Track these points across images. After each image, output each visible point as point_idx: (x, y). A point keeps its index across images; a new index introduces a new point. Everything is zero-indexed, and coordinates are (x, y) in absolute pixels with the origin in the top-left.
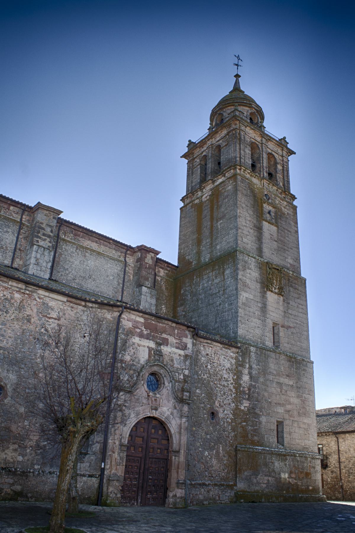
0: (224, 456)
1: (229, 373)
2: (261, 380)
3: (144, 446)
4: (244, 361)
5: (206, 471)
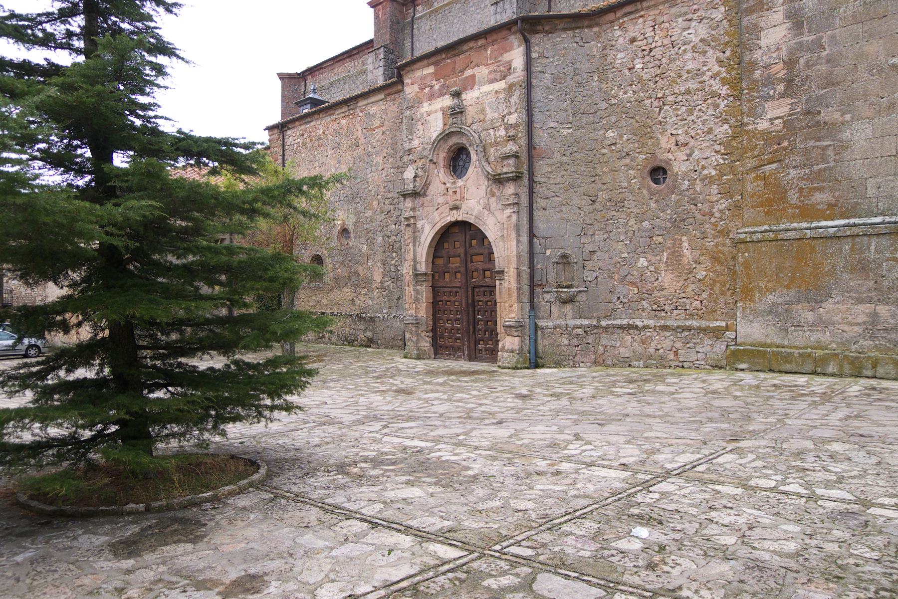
1: (704, 53)
3: (462, 269)
5: (644, 299)
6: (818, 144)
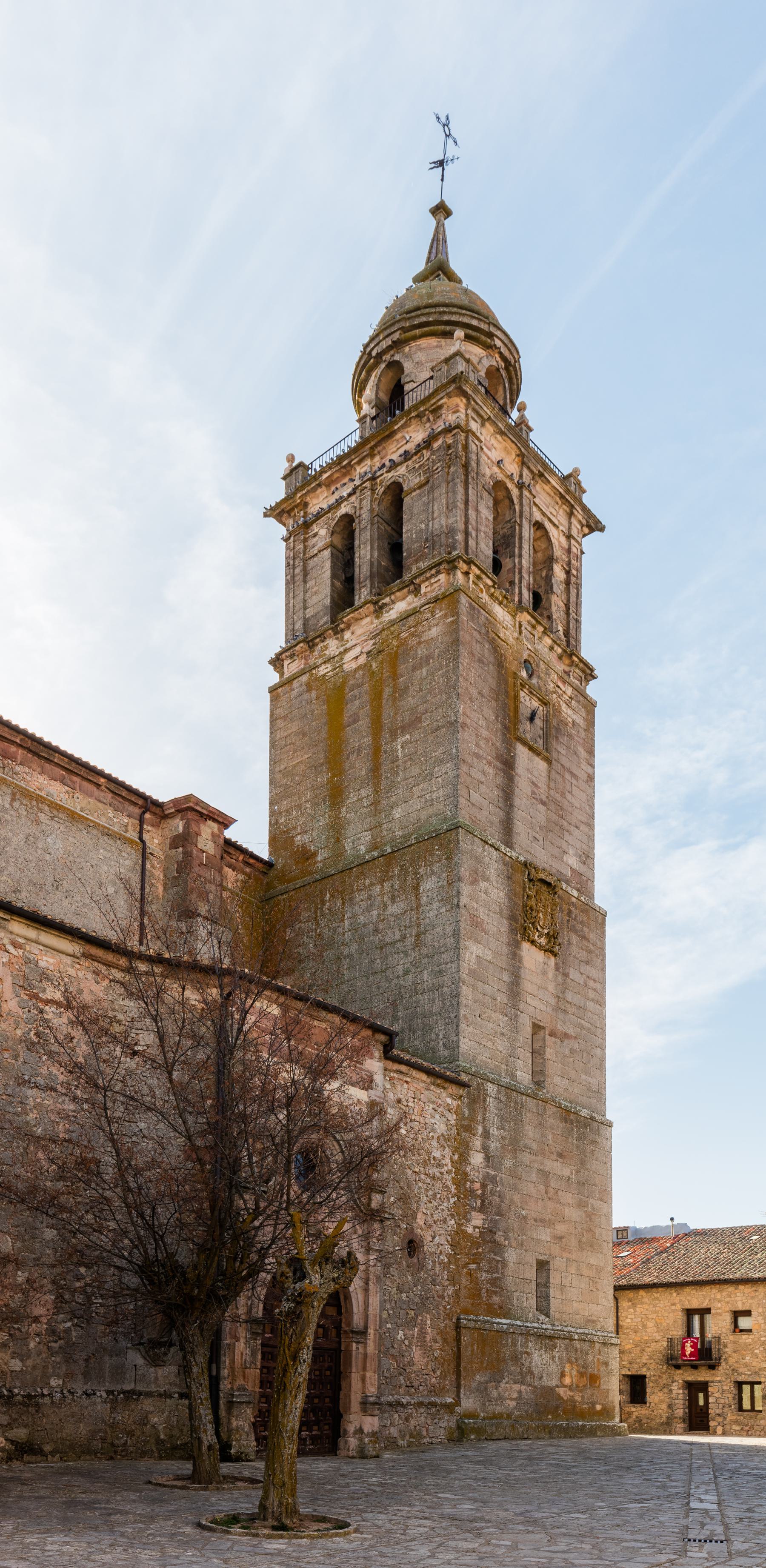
0: (436, 1342)
2: (508, 1163)
4: (472, 1118)
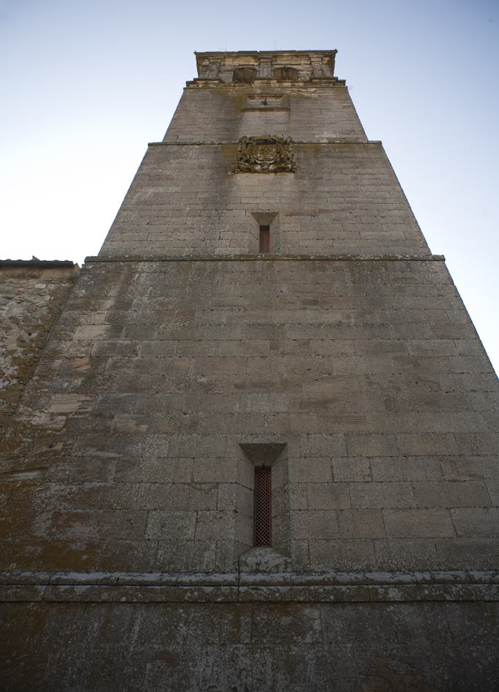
6: (100, 454)
